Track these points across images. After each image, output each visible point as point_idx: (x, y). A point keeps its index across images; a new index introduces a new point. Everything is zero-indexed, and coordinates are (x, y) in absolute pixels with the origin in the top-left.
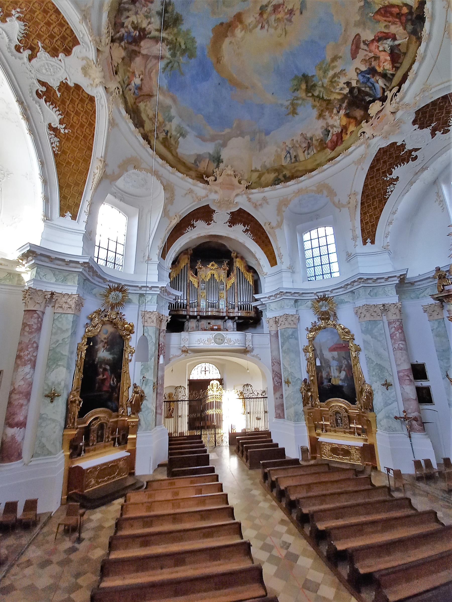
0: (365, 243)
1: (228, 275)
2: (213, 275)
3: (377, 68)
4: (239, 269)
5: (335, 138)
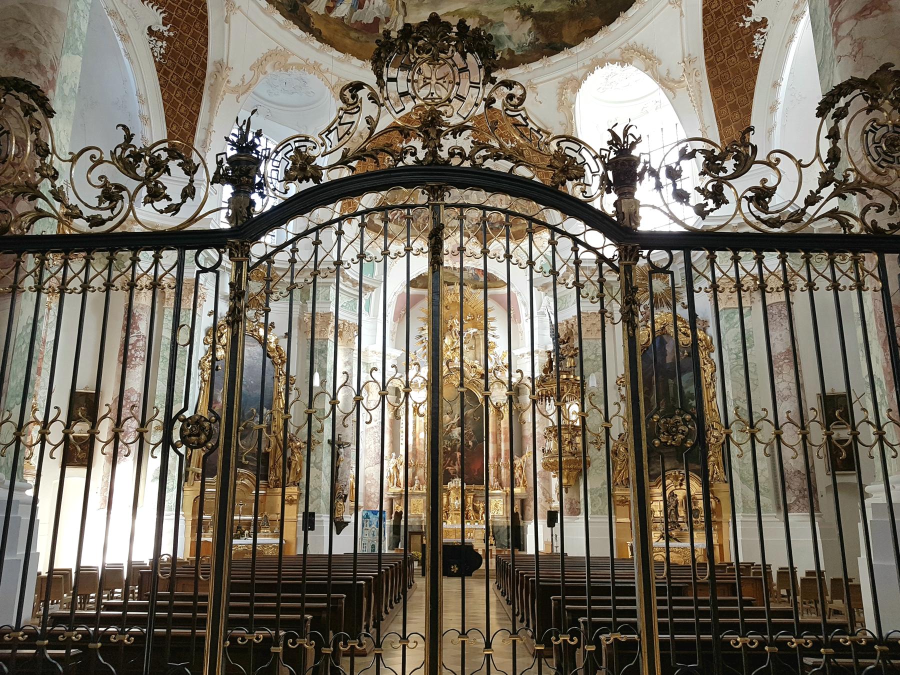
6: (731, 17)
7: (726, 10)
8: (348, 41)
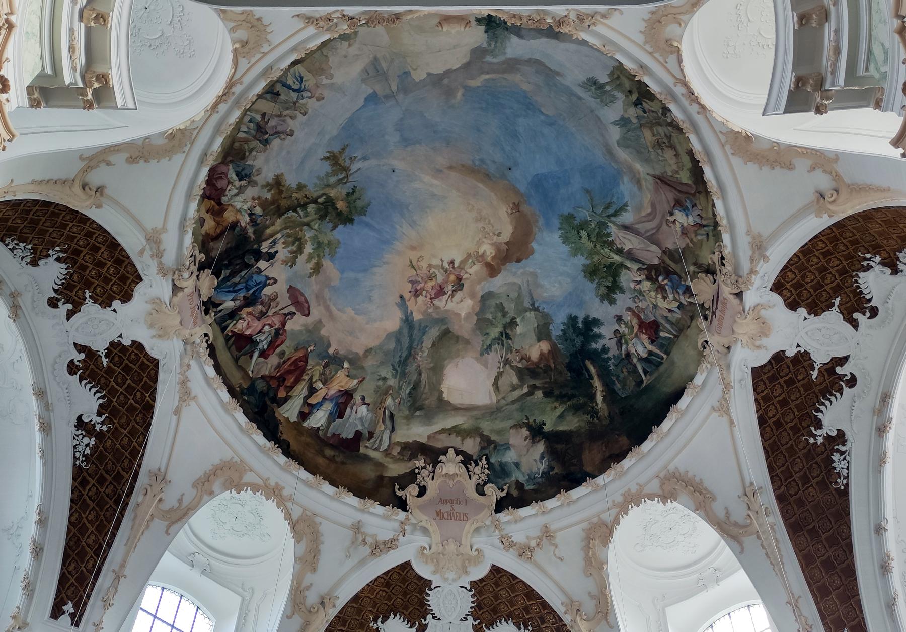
5: (220, 184)
6: (796, 429)
7: (788, 419)
8: (321, 461)
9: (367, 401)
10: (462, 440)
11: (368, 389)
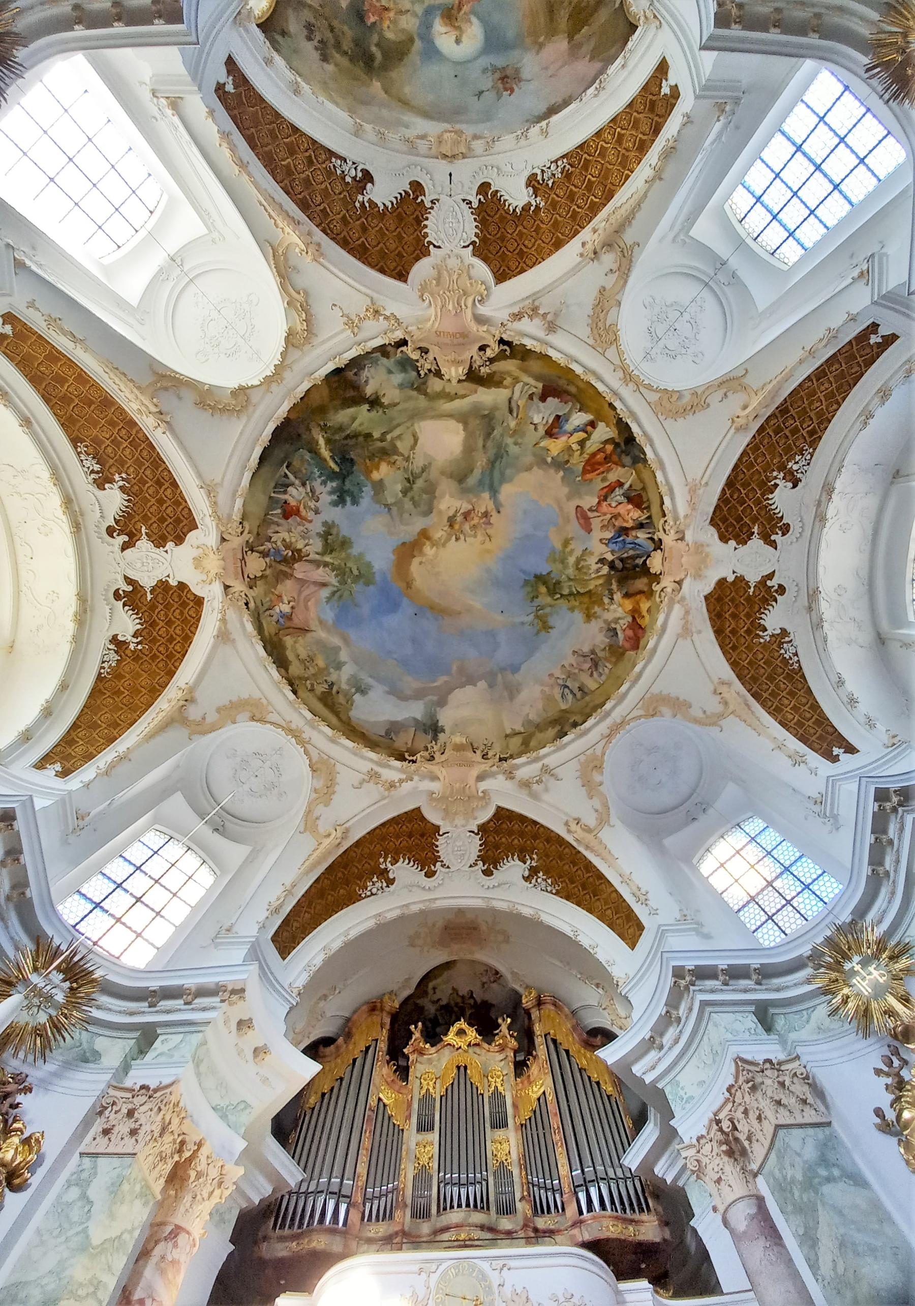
0: (835, 759)
1: (520, 1067)
2: (462, 1069)
3: (625, 525)
4: (554, 1041)
5: (630, 633)
9: (533, 427)
10: (444, 388)
11: (532, 437)
